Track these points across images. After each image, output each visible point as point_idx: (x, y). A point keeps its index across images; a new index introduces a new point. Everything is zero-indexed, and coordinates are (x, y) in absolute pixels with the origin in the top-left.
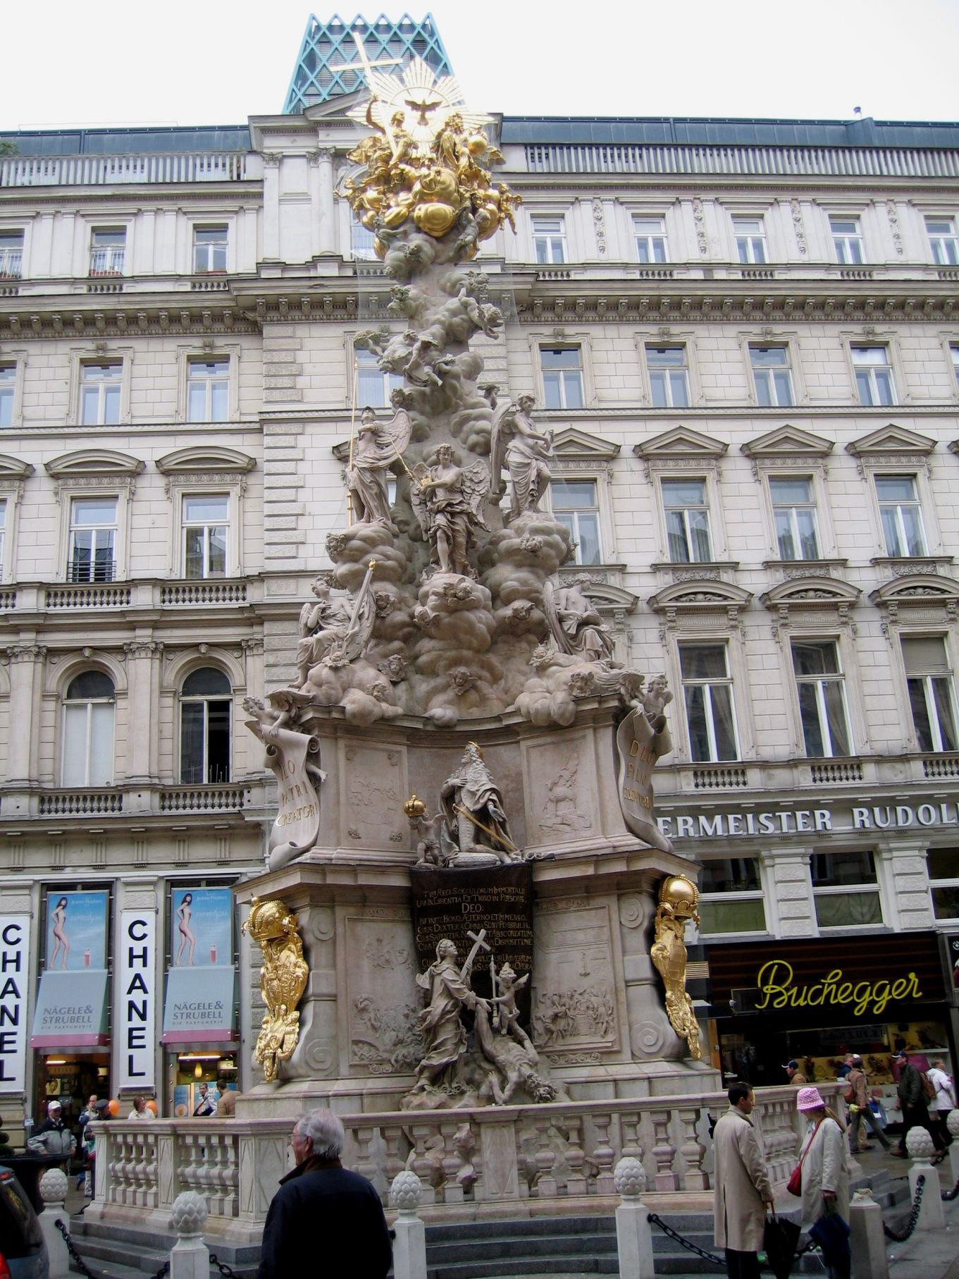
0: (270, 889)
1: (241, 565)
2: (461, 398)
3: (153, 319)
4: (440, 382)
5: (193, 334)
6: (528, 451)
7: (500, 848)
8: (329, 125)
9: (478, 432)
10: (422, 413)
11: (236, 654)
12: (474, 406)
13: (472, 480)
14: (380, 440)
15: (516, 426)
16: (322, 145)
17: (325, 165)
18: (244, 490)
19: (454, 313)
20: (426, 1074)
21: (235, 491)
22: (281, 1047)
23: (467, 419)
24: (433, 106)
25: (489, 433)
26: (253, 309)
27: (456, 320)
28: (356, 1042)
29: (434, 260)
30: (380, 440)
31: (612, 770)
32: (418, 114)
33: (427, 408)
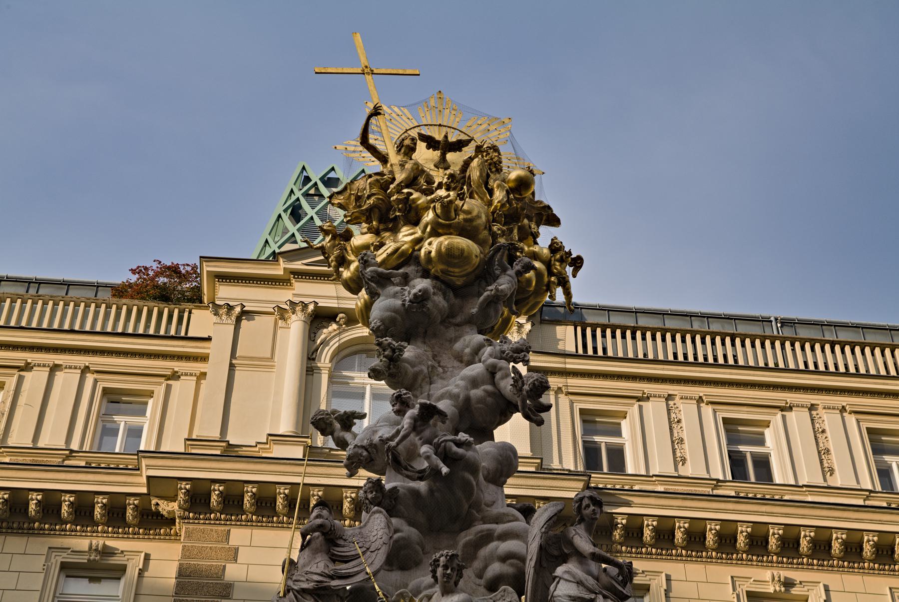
2: (477, 505)
4: (445, 470)
6: (590, 582)
9: (505, 558)
10: (411, 524)
12: (498, 520)
14: (337, 551)
15: (570, 543)
19: (474, 382)
23: (487, 538)
24: (458, 146)
25: (523, 559)
27: (476, 393)
29: (449, 318)
30: (337, 551)
32: (438, 153)
33: (421, 518)
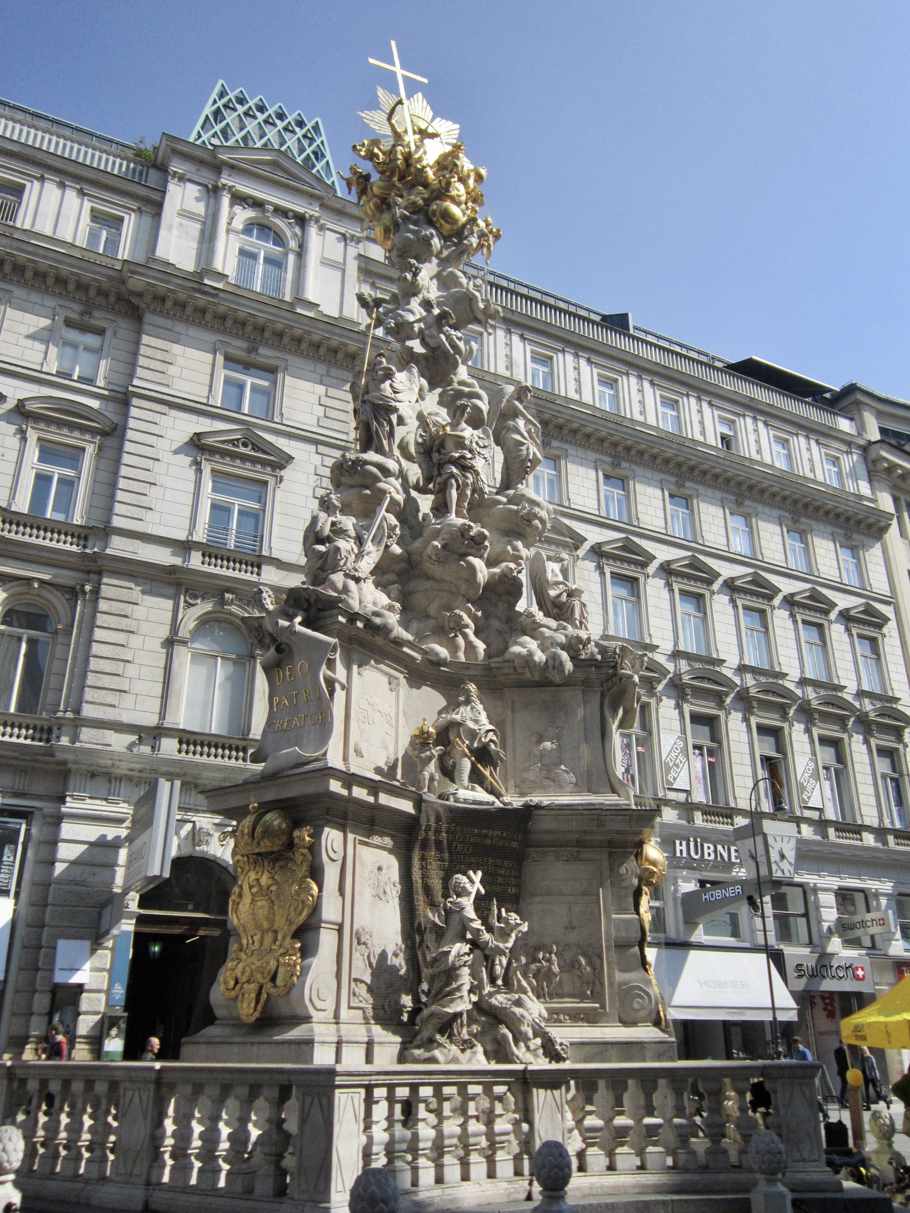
0: (271, 795)
1: (88, 514)
3: (40, 276)
5: (74, 300)
7: (492, 791)
8: (232, 167)
11: (67, 596)
13: (477, 444)
16: (223, 181)
17: (226, 200)
18: (100, 449)
20: (435, 1021)
21: (90, 450)
22: (273, 979)
24: (434, 136)
26: (140, 295)
28: (356, 980)
31: (598, 733)
